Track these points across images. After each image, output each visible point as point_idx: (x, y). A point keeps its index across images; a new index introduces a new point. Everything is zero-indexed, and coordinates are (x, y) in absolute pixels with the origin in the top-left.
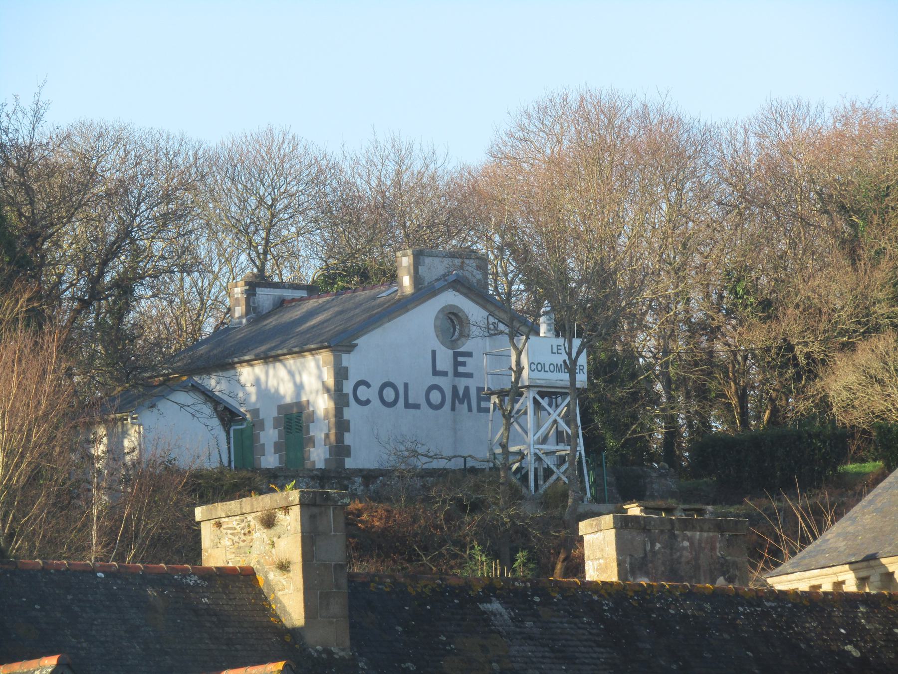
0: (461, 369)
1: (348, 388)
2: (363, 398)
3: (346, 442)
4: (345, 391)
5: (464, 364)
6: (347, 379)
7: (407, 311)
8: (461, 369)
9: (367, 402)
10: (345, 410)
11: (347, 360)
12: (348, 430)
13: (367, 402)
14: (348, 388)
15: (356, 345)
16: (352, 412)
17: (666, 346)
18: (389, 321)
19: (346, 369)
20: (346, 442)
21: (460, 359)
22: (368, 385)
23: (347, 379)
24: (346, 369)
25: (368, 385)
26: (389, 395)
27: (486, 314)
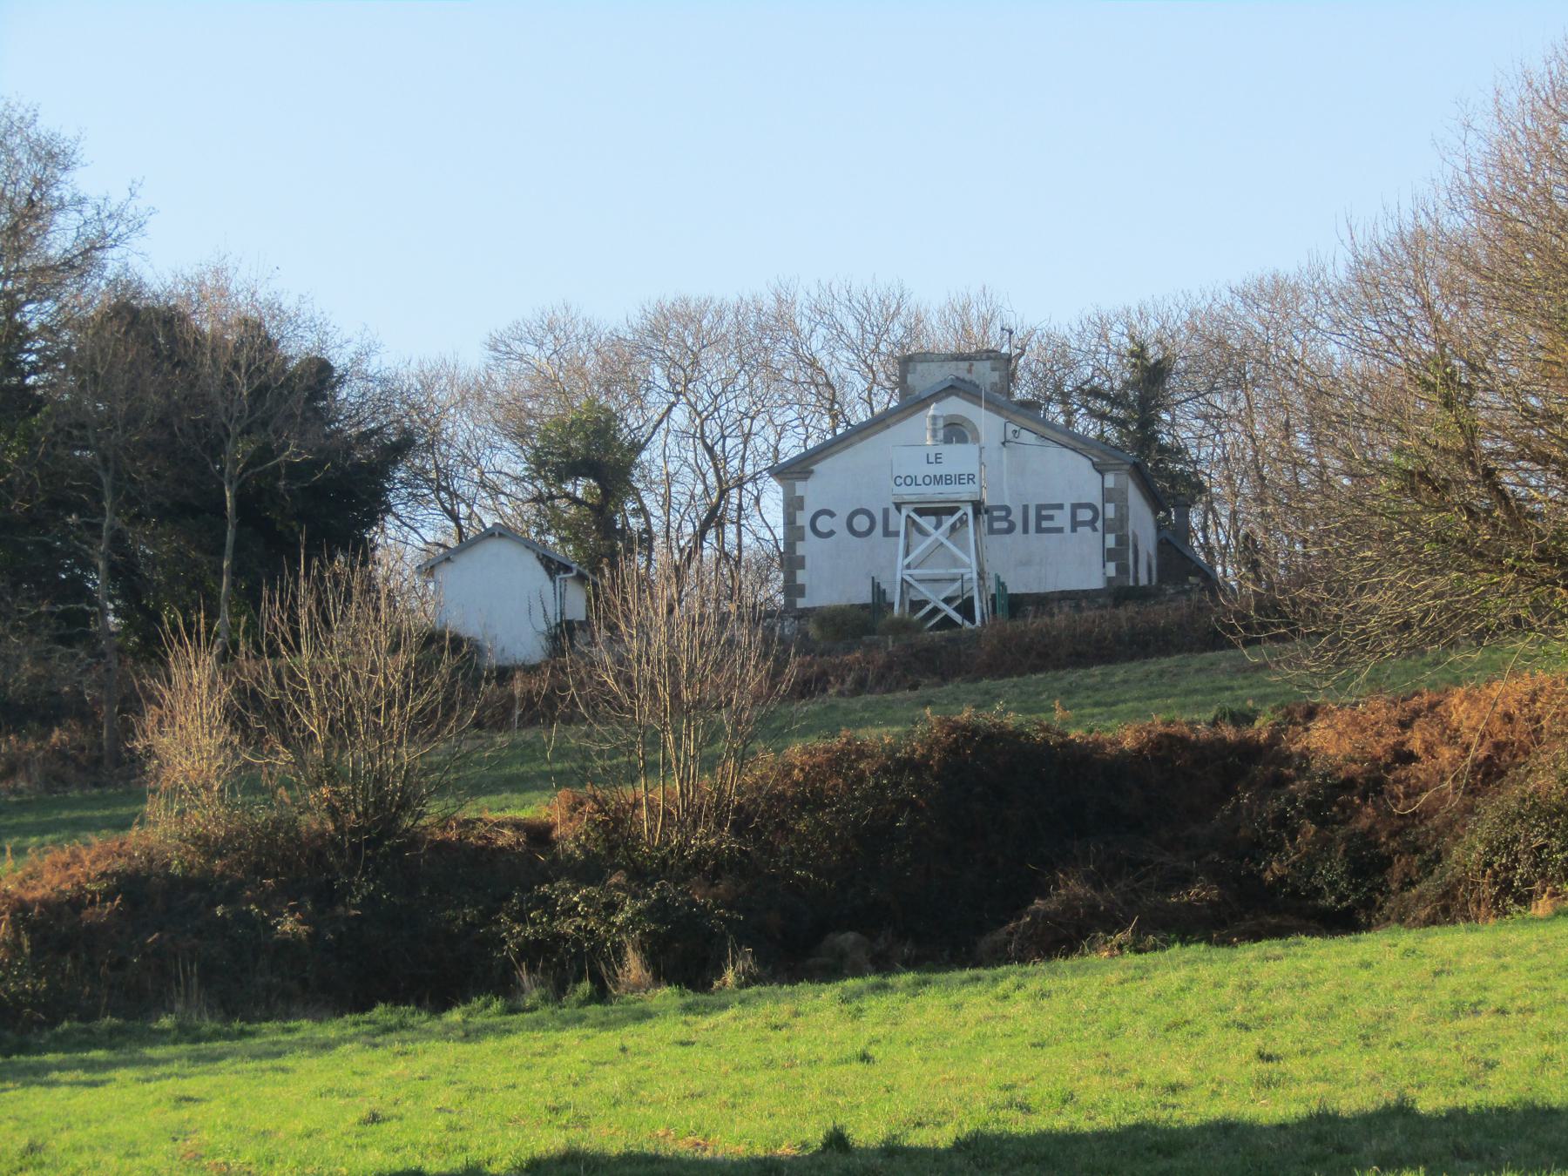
0: (1045, 524)
1: (803, 519)
2: (825, 530)
3: (799, 581)
4: (799, 522)
5: (1051, 518)
6: (802, 508)
7: (888, 427)
8: (1045, 524)
9: (831, 533)
10: (799, 545)
11: (801, 488)
12: (802, 567)
13: (831, 533)
14: (803, 519)
15: (812, 472)
16: (809, 547)
17: (16, 225)
18: (862, 440)
19: (801, 499)
20: (799, 581)
21: (1044, 513)
22: (831, 514)
23: (802, 508)
24: (801, 499)
25: (831, 514)
26: (861, 523)
27: (1003, 420)
